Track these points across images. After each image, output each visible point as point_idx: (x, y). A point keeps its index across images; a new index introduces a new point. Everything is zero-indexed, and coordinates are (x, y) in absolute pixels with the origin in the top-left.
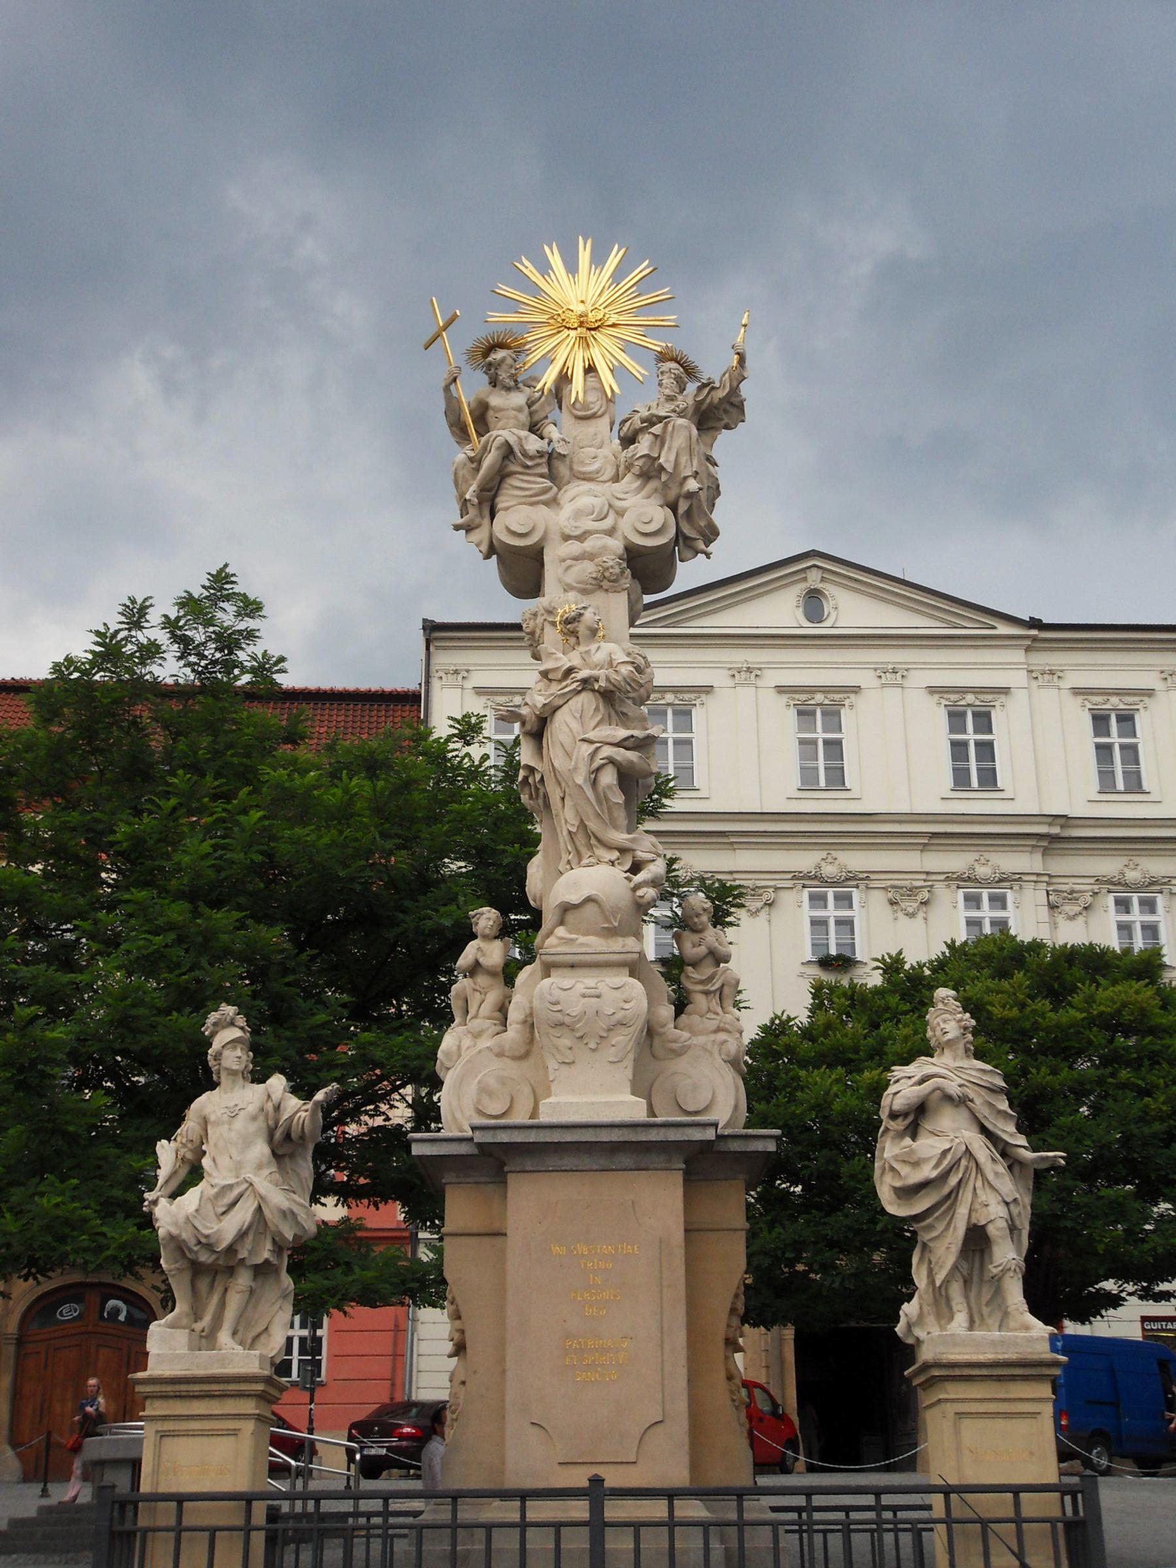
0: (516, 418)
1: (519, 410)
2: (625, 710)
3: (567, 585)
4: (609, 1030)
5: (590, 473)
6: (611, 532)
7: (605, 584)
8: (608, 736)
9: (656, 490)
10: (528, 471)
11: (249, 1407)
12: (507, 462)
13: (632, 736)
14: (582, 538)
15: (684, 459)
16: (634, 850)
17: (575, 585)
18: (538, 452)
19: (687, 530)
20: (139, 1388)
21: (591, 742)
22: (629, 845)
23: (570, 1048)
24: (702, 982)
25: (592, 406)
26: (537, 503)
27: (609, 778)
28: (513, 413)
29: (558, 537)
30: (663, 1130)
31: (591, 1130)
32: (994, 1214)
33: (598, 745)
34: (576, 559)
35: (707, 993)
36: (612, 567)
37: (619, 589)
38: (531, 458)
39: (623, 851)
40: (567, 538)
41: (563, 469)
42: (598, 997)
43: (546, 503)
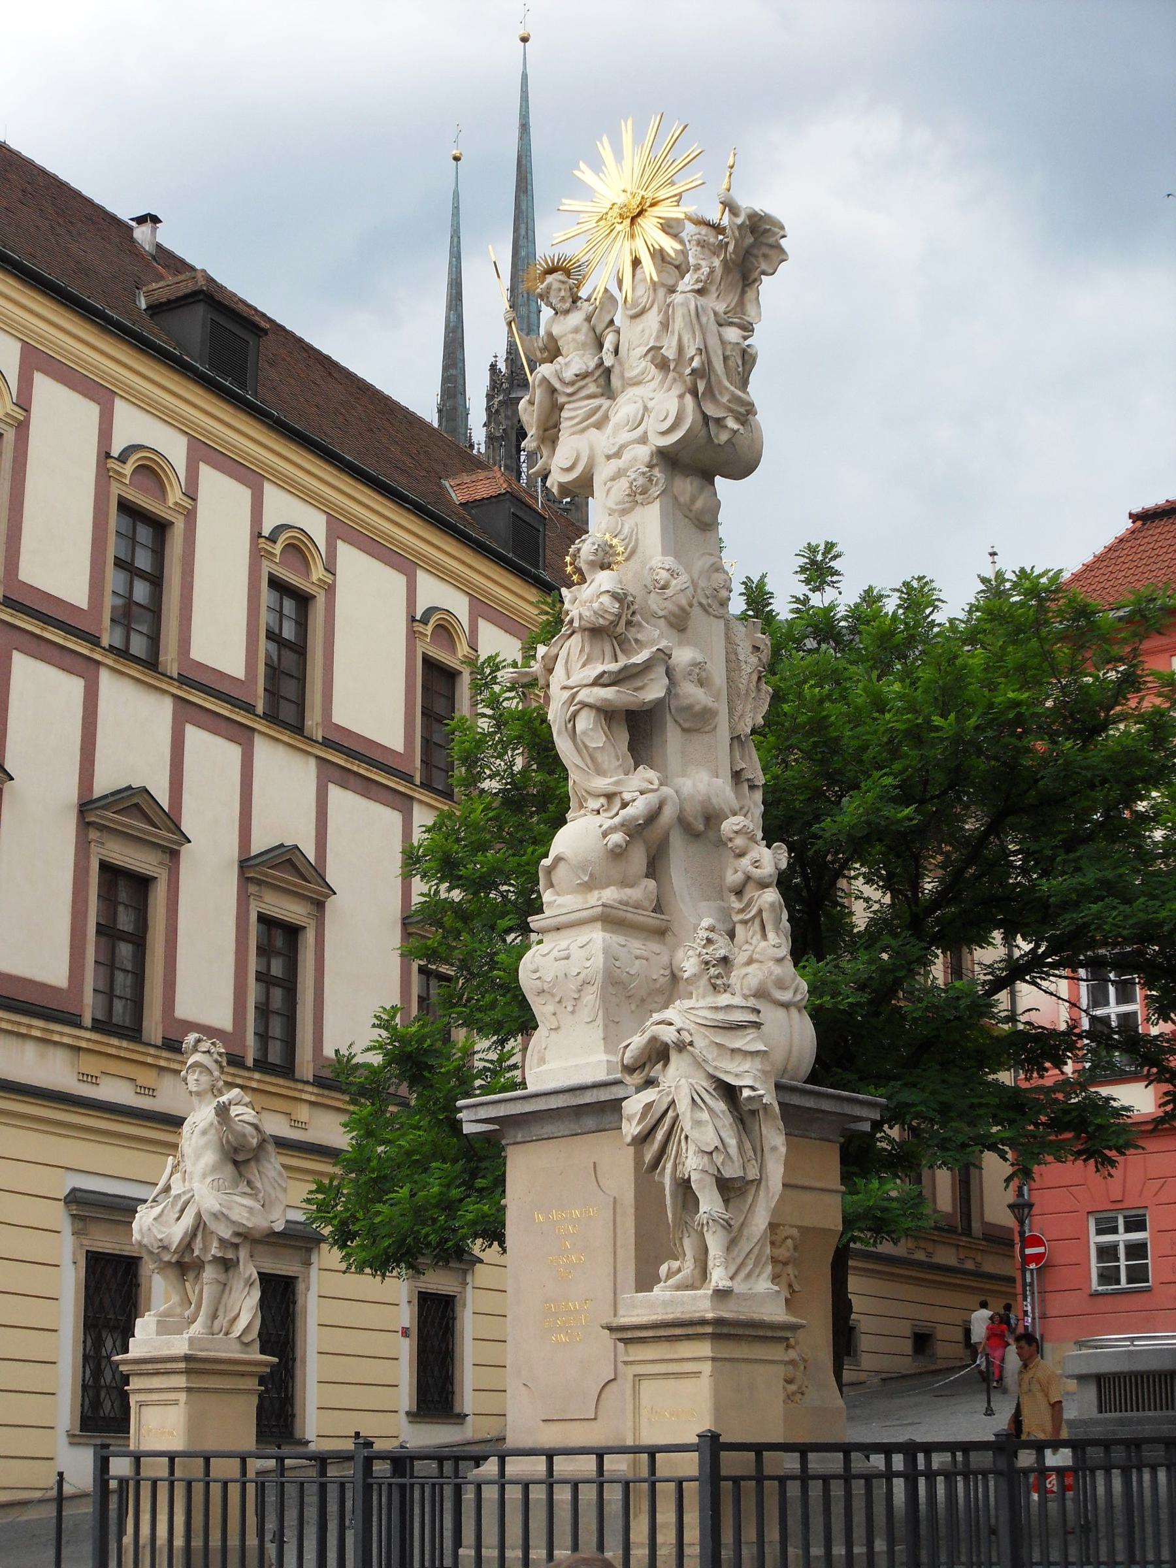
0: (574, 340)
1: (576, 330)
2: (639, 636)
3: (610, 509)
4: (580, 991)
5: (635, 377)
6: (643, 440)
7: (639, 498)
8: (583, 678)
9: (675, 380)
10: (571, 399)
11: (181, 1381)
12: (556, 395)
13: (604, 672)
14: (618, 455)
15: (686, 338)
16: (620, 793)
17: (615, 507)
18: (577, 375)
19: (711, 411)
20: (121, 1368)
21: (572, 688)
22: (612, 789)
23: (554, 1014)
24: (742, 911)
25: (640, 301)
26: (587, 428)
27: (584, 722)
28: (570, 336)
29: (603, 459)
30: (595, 1091)
31: (543, 1099)
32: (692, 1164)
33: (575, 690)
34: (613, 479)
35: (745, 922)
36: (635, 480)
37: (650, 500)
38: (572, 383)
39: (610, 797)
40: (609, 457)
41: (616, 382)
42: (567, 958)
43: (599, 426)
